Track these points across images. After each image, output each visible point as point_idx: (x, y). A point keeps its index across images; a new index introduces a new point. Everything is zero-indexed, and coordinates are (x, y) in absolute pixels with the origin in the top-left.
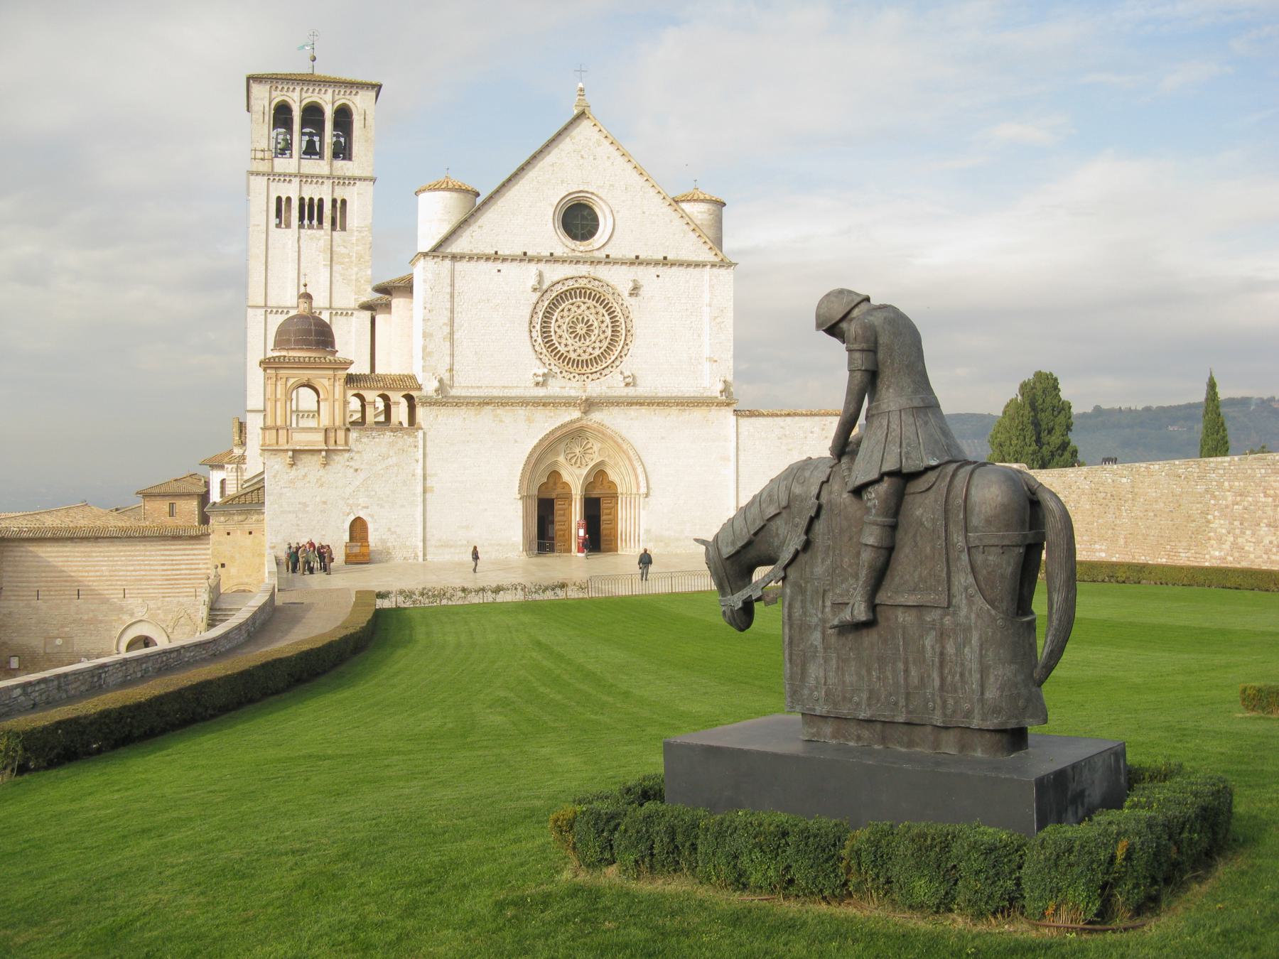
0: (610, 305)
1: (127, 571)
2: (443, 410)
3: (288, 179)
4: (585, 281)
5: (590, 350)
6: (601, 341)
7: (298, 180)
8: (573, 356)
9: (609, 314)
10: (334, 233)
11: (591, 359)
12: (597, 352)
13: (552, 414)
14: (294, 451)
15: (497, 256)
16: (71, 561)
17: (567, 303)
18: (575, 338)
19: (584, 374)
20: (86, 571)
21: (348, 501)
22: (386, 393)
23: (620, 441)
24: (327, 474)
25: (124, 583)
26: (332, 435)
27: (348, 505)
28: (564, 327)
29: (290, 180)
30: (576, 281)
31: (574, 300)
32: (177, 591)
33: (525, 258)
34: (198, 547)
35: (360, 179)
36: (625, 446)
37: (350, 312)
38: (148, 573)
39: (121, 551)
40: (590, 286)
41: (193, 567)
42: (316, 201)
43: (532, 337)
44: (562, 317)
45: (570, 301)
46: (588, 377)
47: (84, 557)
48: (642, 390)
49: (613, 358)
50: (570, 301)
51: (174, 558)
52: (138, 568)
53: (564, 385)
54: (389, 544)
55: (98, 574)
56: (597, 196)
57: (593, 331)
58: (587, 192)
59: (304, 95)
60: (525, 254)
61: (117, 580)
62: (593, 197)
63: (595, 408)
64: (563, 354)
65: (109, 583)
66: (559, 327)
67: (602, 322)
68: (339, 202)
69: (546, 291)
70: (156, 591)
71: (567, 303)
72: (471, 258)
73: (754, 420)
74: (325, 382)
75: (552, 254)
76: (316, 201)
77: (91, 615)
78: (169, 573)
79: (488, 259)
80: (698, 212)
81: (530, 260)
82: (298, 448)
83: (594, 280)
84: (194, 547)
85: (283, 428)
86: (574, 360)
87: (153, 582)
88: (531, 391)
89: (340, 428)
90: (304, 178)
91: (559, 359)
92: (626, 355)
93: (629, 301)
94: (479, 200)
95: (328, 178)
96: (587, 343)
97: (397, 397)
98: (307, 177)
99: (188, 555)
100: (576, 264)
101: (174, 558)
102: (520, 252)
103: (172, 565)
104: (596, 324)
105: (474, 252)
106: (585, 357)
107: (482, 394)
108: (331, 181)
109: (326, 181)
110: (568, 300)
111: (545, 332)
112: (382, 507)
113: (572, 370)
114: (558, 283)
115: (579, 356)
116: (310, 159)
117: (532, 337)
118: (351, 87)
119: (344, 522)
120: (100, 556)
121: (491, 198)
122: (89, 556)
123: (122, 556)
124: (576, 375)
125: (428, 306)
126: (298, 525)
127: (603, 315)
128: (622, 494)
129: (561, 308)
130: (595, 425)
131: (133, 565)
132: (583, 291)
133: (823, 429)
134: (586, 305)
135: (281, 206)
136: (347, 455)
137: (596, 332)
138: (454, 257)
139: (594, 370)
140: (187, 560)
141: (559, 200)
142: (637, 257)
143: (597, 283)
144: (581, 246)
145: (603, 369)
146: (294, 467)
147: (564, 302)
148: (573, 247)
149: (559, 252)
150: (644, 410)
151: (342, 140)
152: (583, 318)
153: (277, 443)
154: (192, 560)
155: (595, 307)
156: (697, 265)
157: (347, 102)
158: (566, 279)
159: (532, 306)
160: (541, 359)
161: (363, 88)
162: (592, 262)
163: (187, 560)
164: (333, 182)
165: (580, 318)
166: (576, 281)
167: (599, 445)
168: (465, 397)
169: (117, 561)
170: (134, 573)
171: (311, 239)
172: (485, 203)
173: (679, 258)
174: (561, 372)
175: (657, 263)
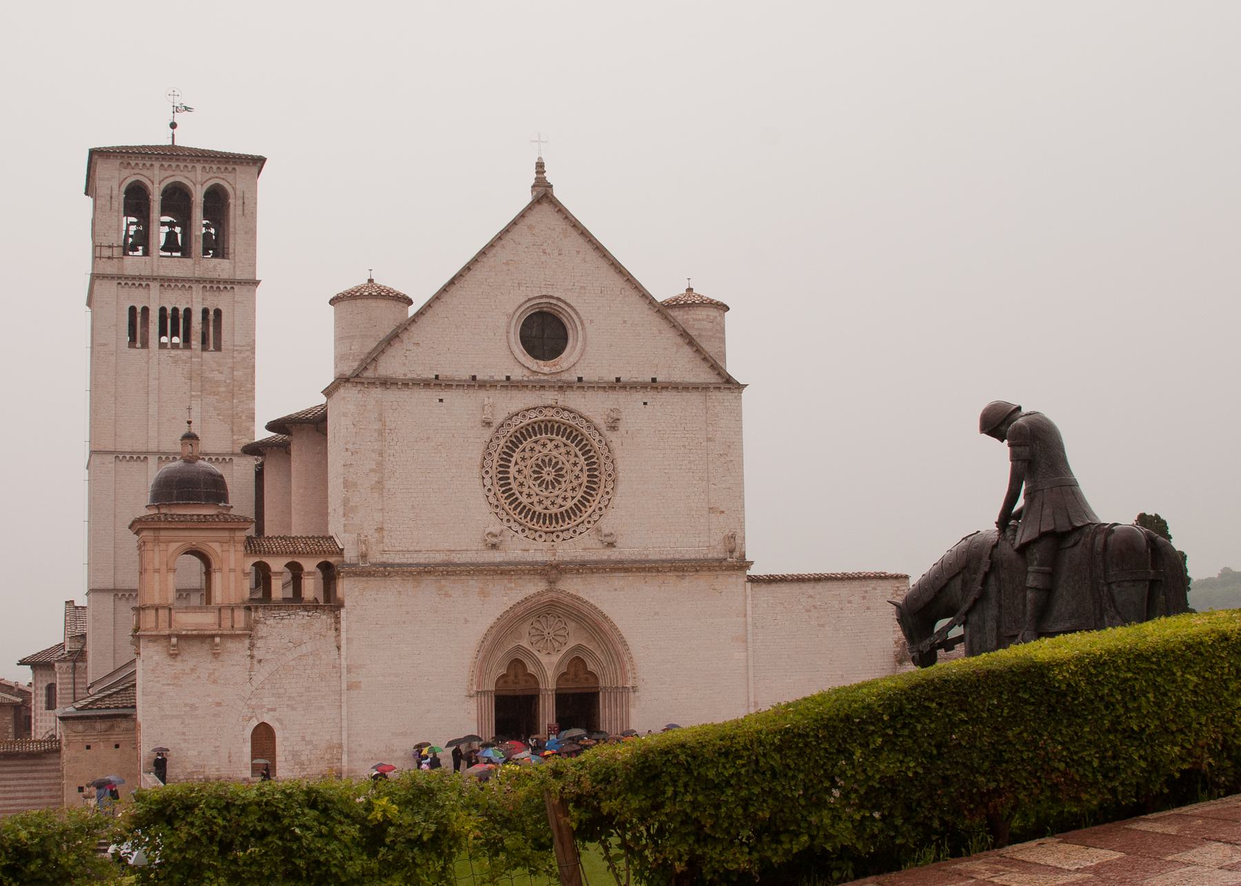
0: (584, 442)
2: (373, 582)
3: (144, 284)
4: (553, 412)
5: (559, 501)
6: (573, 489)
7: (157, 284)
8: (539, 509)
9: (583, 455)
10: (206, 354)
11: (561, 513)
12: (569, 504)
13: (513, 585)
14: (179, 637)
15: (438, 382)
17: (529, 440)
18: (540, 485)
19: (552, 533)
21: (248, 702)
22: (296, 560)
23: (600, 619)
24: (222, 666)
26: (226, 614)
27: (249, 706)
29: (148, 285)
30: (541, 412)
31: (539, 436)
33: (474, 383)
34: (40, 768)
35: (240, 283)
36: (606, 627)
37: (227, 459)
40: (558, 419)
41: (33, 794)
42: (181, 312)
43: (484, 486)
44: (523, 459)
45: (534, 438)
46: (558, 536)
48: (627, 550)
49: (590, 510)
50: (534, 438)
51: (8, 783)
53: (527, 547)
54: (303, 758)
56: (565, 303)
57: (562, 476)
58: (552, 297)
60: (474, 378)
62: (560, 304)
63: (568, 576)
64: (525, 507)
66: (519, 471)
67: (575, 464)
68: (211, 313)
69: (502, 426)
71: (529, 440)
72: (406, 385)
73: (773, 587)
74: (216, 546)
75: (508, 378)
76: (181, 312)
79: (426, 384)
80: (694, 320)
81: (483, 385)
82: (184, 633)
83: (564, 410)
84: (34, 768)
85: (163, 607)
86: (540, 514)
88: (485, 555)
89: (239, 607)
90: (166, 282)
91: (520, 513)
92: (606, 506)
93: (610, 435)
94: (412, 310)
95: (198, 281)
96: (556, 492)
97: (309, 565)
98: (170, 280)
99: (26, 779)
100: (539, 390)
101: (8, 783)
102: (465, 375)
104: (568, 466)
105: (409, 376)
107: (422, 561)
108: (202, 286)
109: (194, 286)
110: (531, 437)
111: (504, 480)
112: (293, 709)
113: (537, 527)
114: (517, 415)
115: (546, 508)
116: (171, 257)
117: (484, 486)
118: (228, 162)
119: (244, 730)
121: (429, 305)
124: (543, 535)
125: (350, 446)
126: (184, 734)
127: (576, 456)
128: (605, 688)
129: (521, 446)
130: (568, 599)
132: (549, 425)
133: (864, 598)
134: (554, 442)
135: (137, 319)
136: (247, 642)
137: (567, 478)
139: (566, 527)
140: (25, 785)
141: (515, 308)
142: (618, 380)
143: (566, 414)
144: (545, 367)
145: (577, 526)
146: (179, 658)
147: (526, 440)
148: (535, 368)
149: (517, 374)
150: (630, 578)
151: (213, 231)
152: (550, 460)
153: (157, 627)
154: (33, 785)
155: (565, 445)
156: (695, 388)
157: (221, 182)
158: (527, 410)
159: (483, 448)
160: (497, 514)
161: (242, 163)
162: (561, 387)
163: (25, 785)
164: (204, 287)
165: (547, 460)
166: (541, 412)
167: (573, 624)
168: (400, 565)
171: (176, 362)
172: (420, 313)
173: (672, 379)
174: (523, 531)
175: (644, 386)
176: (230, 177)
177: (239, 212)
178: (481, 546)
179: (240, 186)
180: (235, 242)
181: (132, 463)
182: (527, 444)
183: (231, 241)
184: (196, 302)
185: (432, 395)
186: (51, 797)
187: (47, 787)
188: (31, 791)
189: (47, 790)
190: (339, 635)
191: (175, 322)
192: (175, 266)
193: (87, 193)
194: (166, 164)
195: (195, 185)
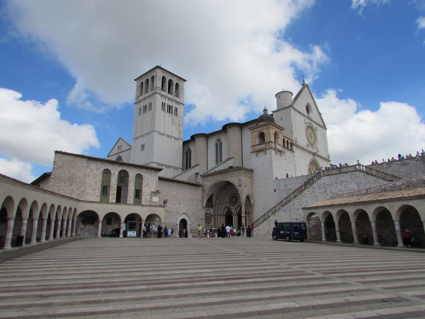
1: (181, 195)
16: (166, 189)
20: (170, 193)
25: (180, 199)
28: (309, 134)
32: (193, 204)
34: (198, 189)
38: (186, 196)
39: (179, 188)
47: (169, 188)
52: (183, 194)
55: (173, 194)
58: (309, 103)
59: (170, 77)
61: (178, 198)
65: (175, 198)
70: (188, 203)
77: (170, 210)
78: (191, 197)
84: (197, 189)
87: (187, 200)
90: (169, 99)
98: (170, 99)
99: (196, 192)
103: (192, 194)
106: (312, 143)
109: (174, 102)
120: (173, 188)
122: (170, 188)
123: (179, 189)
131: (182, 193)
135: (163, 104)
138: (296, 110)
149: (307, 116)
169: (178, 191)
170: (182, 196)
176: (180, 82)
177: (181, 89)
178: (306, 146)
179: (182, 85)
180: (181, 95)
181: (161, 135)
182: (308, 129)
183: (180, 95)
184: (174, 105)
185: (298, 114)
186: (200, 197)
187: (200, 195)
188: (196, 195)
189: (200, 195)
190: (294, 158)
191: (170, 107)
192: (169, 96)
193: (135, 80)
194: (170, 75)
195: (174, 81)
